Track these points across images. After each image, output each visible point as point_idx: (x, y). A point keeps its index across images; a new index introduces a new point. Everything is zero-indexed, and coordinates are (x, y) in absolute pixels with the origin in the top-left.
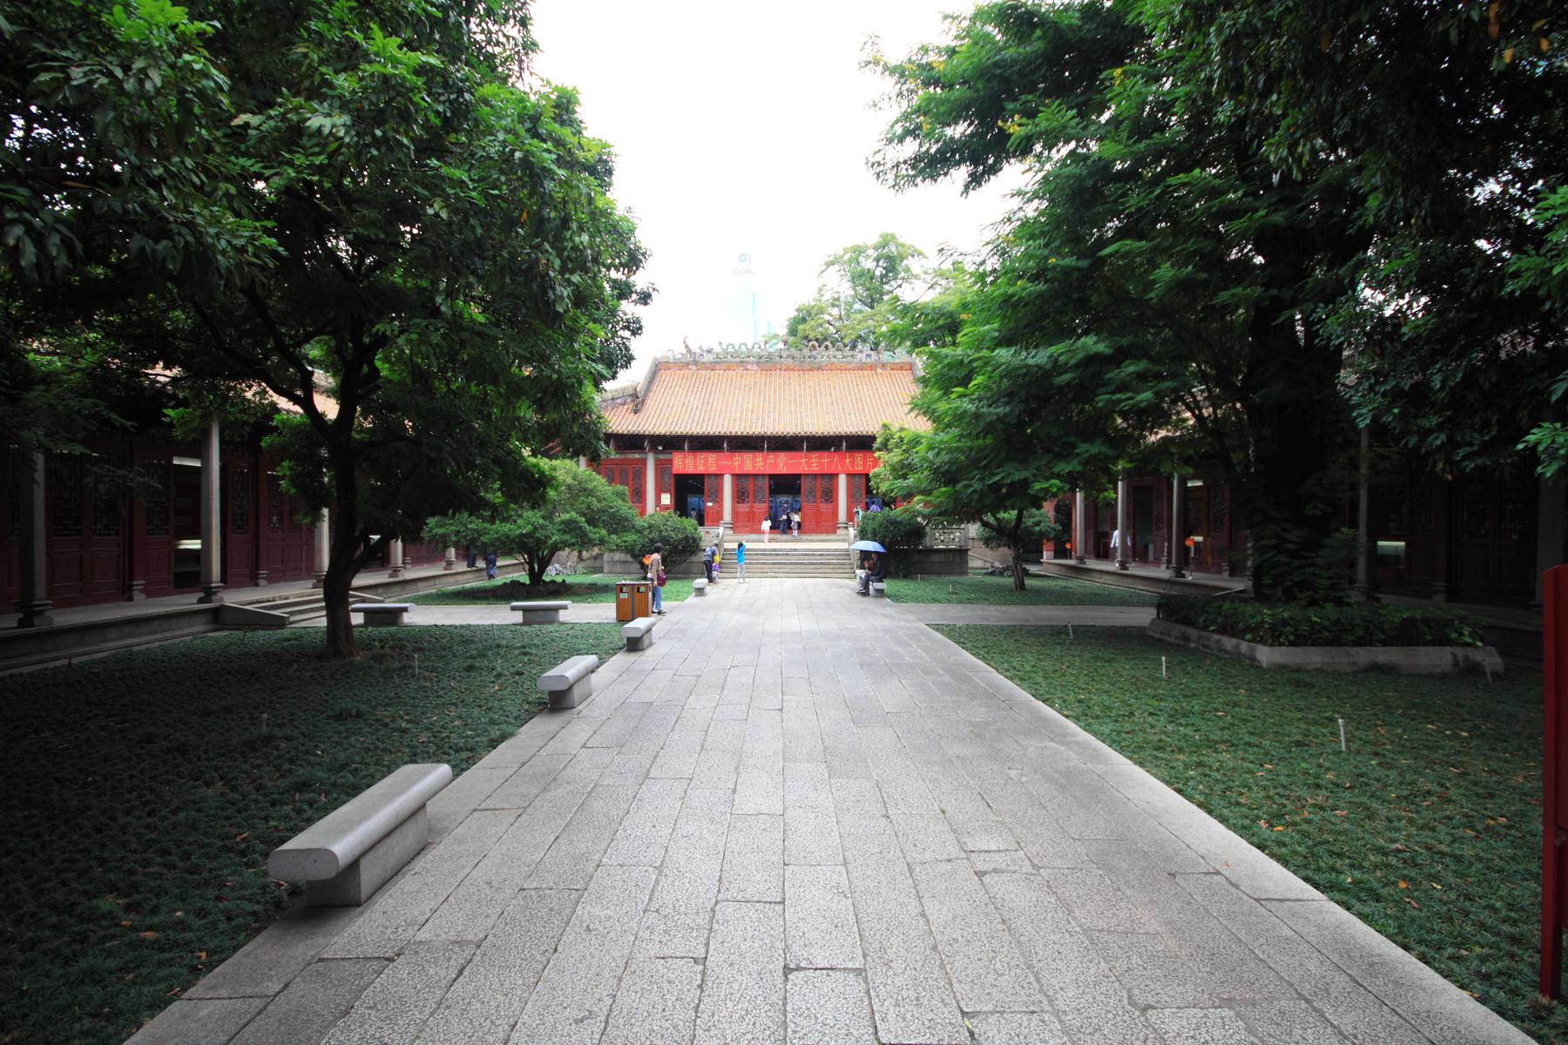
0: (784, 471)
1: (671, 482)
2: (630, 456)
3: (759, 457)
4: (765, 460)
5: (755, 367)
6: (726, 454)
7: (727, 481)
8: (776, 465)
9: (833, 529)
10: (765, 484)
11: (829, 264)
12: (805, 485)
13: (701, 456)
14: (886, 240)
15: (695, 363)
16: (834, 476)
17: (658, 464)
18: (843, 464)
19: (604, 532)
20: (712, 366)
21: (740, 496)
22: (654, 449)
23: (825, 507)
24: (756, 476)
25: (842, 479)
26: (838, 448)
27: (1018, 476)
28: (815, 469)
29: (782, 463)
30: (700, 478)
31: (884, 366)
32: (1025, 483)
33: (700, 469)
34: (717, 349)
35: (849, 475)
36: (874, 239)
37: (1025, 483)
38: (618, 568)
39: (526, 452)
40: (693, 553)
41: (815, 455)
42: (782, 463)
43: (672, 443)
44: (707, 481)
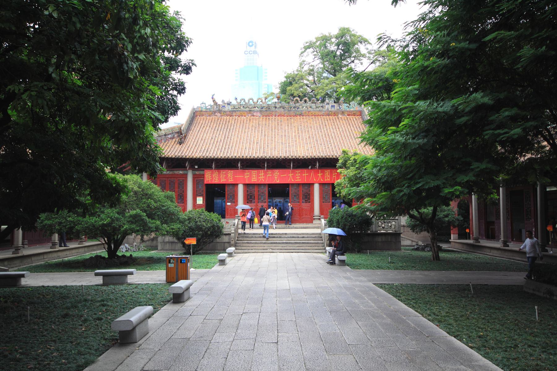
0: (278, 182)
1: (203, 189)
2: (176, 172)
3: (262, 173)
4: (265, 174)
5: (259, 114)
6: (240, 170)
7: (241, 188)
8: (273, 177)
9: (311, 220)
10: (266, 190)
11: (306, 48)
13: (223, 172)
14: (344, 32)
15: (220, 111)
16: (311, 185)
17: (195, 177)
18: (317, 178)
19: (158, 222)
22: (192, 167)
23: (305, 206)
24: (259, 185)
25: (316, 187)
26: (313, 167)
27: (433, 184)
28: (298, 180)
29: (277, 177)
31: (343, 113)
32: (438, 189)
33: (223, 181)
34: (234, 102)
35: (321, 185)
36: (335, 32)
37: (438, 189)
38: (167, 246)
39: (107, 170)
40: (218, 236)
41: (298, 171)
42: (277, 177)
43: (204, 164)
44: (227, 189)
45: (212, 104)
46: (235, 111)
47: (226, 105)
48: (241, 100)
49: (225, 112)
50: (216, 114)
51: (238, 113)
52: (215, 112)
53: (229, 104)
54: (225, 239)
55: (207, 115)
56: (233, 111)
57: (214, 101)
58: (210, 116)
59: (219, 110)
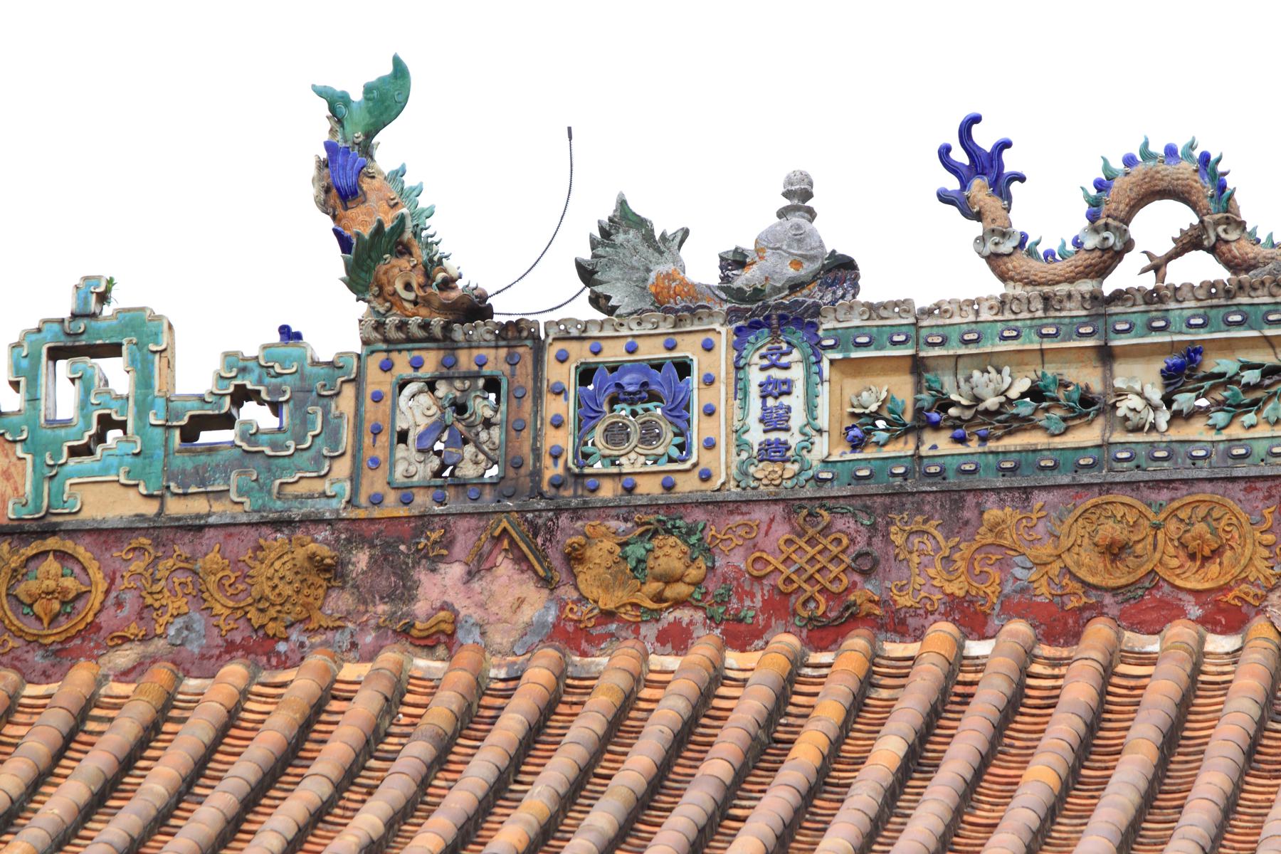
15: (534, 522)
20: (829, 561)
34: (919, 260)
45: (337, 325)
46: (953, 497)
47: (711, 352)
48: (1113, 206)
49: (665, 517)
50: (440, 587)
51: (1049, 544)
52: (402, 545)
53: (793, 301)
55: (181, 620)
56: (884, 500)
57: (380, 250)
58: (262, 648)
59: (519, 481)
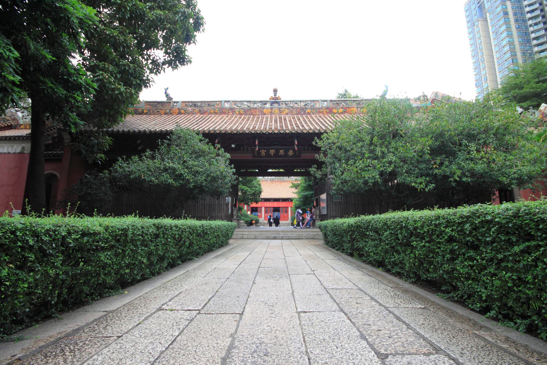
3: (270, 203)
7: (263, 208)
10: (272, 209)
12: (281, 209)
16: (287, 207)
21: (266, 212)
23: (286, 214)
28: (283, 206)
29: (276, 204)
30: (256, 208)
41: (283, 203)
42: (276, 204)
54: (260, 224)
